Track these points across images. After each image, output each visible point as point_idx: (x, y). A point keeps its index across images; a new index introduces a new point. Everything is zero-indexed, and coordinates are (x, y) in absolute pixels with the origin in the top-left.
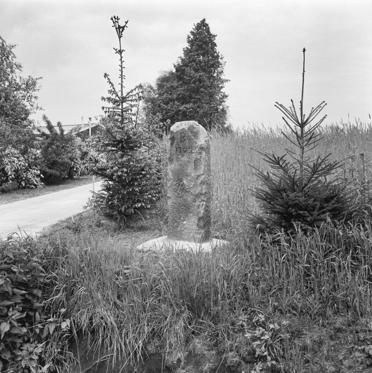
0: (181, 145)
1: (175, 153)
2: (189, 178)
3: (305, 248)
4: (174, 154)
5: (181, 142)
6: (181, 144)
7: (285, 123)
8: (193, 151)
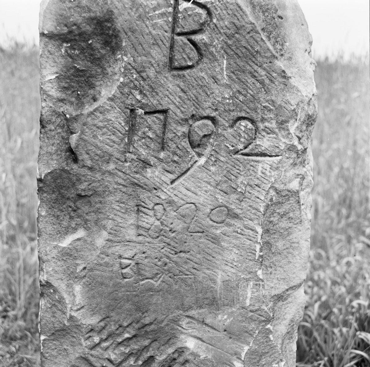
0: (169, 91)
1: (115, 150)
2: (223, 318)
3: (149, 243)
4: (107, 158)
5: (174, 67)
6: (170, 83)
7: (184, 177)
8: (264, 143)
